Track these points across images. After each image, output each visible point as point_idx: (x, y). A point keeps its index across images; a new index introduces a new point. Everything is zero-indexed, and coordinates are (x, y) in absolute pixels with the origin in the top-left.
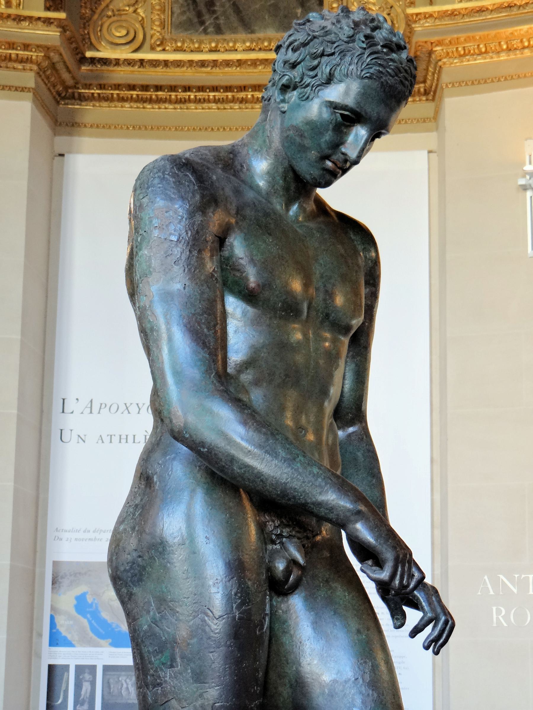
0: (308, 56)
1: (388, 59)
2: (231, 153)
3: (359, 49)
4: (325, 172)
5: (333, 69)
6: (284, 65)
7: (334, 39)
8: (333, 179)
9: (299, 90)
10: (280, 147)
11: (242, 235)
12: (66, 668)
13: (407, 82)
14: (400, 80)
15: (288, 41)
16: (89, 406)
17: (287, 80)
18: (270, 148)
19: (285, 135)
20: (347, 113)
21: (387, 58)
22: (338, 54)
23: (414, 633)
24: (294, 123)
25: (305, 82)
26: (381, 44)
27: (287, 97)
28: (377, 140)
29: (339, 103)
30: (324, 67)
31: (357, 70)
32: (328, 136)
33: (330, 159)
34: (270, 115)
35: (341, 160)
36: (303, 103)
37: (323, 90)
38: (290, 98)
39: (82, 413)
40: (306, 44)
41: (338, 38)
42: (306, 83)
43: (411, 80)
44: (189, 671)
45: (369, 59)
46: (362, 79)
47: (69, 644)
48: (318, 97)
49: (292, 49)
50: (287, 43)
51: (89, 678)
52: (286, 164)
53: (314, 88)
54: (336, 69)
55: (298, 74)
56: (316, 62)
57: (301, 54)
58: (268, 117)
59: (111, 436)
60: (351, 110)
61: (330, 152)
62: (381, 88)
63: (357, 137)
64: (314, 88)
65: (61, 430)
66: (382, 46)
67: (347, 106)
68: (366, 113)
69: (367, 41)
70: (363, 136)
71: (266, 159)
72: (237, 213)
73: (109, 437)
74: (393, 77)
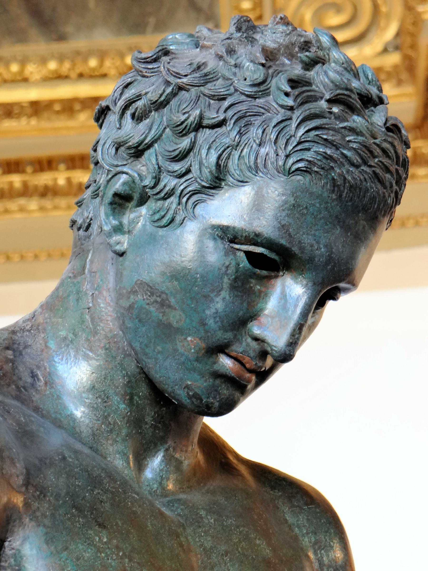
0: (168, 130)
1: (344, 128)
2: (8, 348)
3: (279, 109)
4: (218, 382)
5: (225, 155)
6: (117, 149)
7: (223, 91)
8: (237, 394)
9: (152, 204)
10: (117, 331)
11: (41, 530)
13: (388, 176)
14: (374, 172)
15: (123, 98)
17: (124, 184)
18: (95, 333)
19: (125, 303)
21: (341, 125)
22: (233, 121)
24: (145, 277)
25: (165, 186)
26: (327, 96)
27: (125, 221)
28: (330, 304)
29: (243, 230)
30: (204, 152)
31: (277, 155)
33: (227, 351)
34: (92, 261)
35: (252, 354)
36: (161, 232)
37: (204, 201)
38: (134, 222)
40: (162, 103)
41: (232, 90)
42: (167, 189)
43: (397, 170)
45: (302, 131)
46: (289, 174)
48: (195, 217)
49: (133, 116)
50: (121, 103)
52: (132, 367)
53: (185, 199)
54: (230, 155)
55: (148, 169)
56: (185, 143)
57: (152, 125)
58: (88, 266)
61: (229, 335)
62: (333, 191)
63: (286, 301)
64: (185, 199)
66: (329, 101)
67: (257, 235)
68: (302, 249)
69: (296, 92)
70: (298, 299)
71: (87, 358)
72: (27, 484)
74: (357, 167)
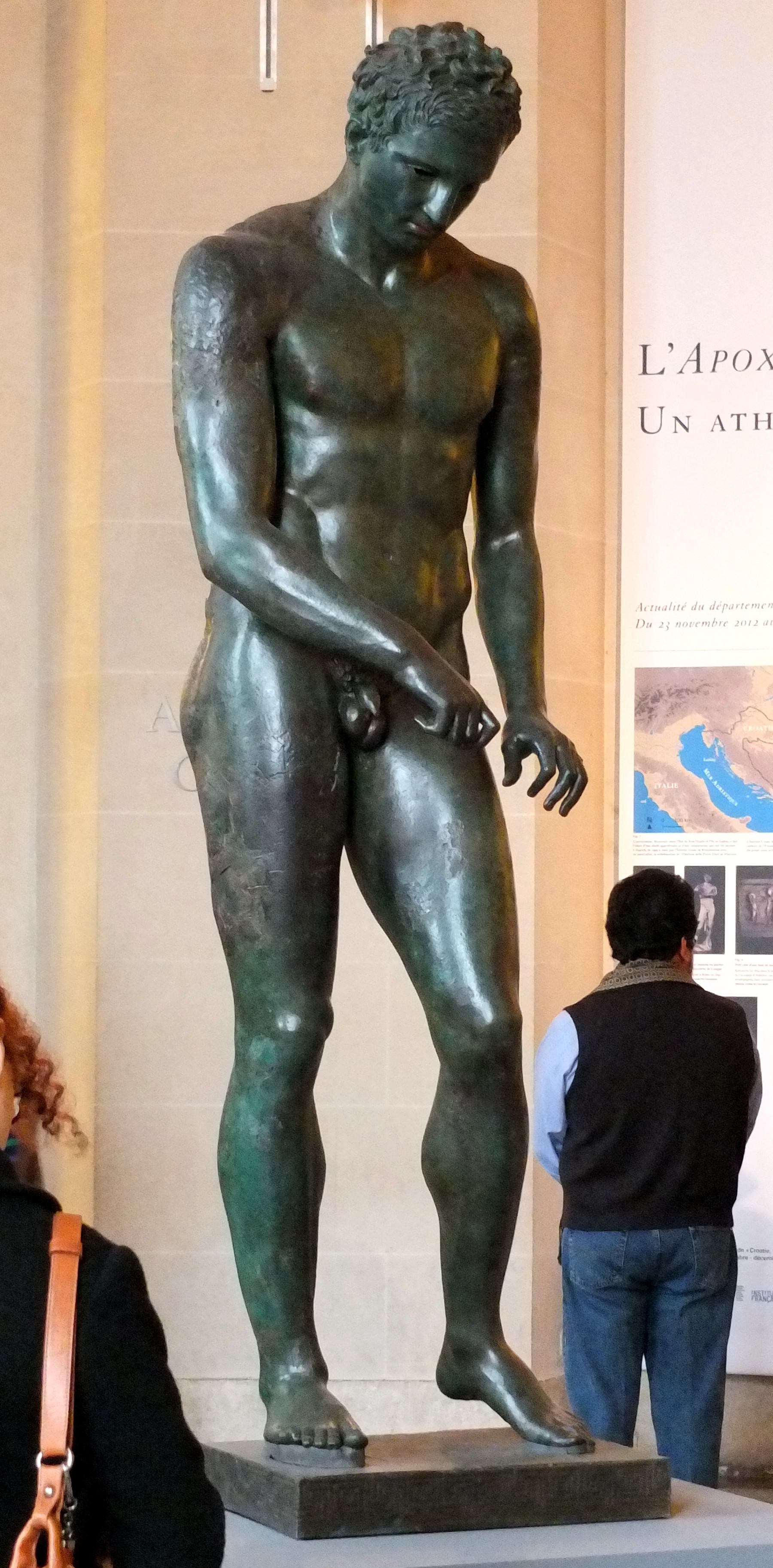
12: (717, 874)
16: (694, 357)
20: (419, 168)
23: (534, 791)
32: (402, 196)
39: (681, 372)
44: (242, 836)
45: (435, 104)
47: (673, 827)
51: (712, 891)
59: (738, 416)
60: (423, 164)
65: (643, 409)
73: (735, 417)
74: (469, 120)
